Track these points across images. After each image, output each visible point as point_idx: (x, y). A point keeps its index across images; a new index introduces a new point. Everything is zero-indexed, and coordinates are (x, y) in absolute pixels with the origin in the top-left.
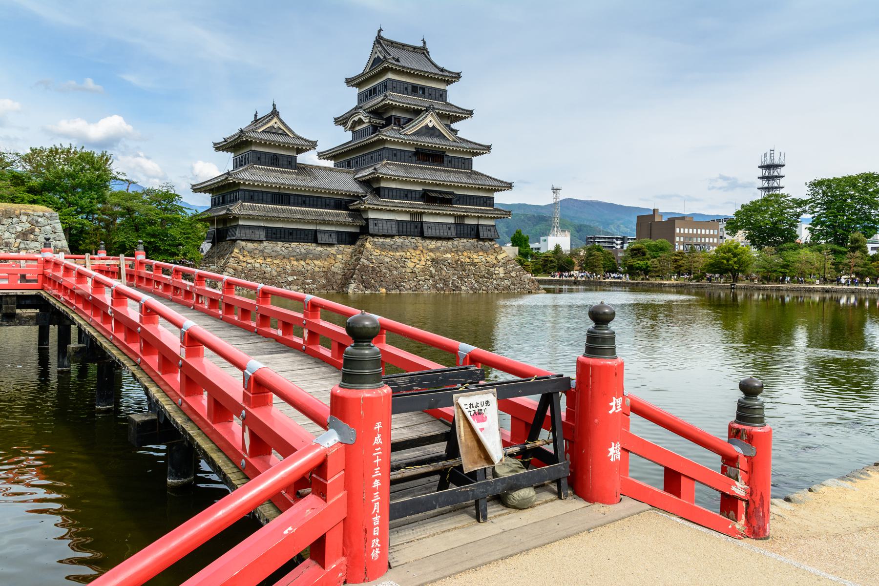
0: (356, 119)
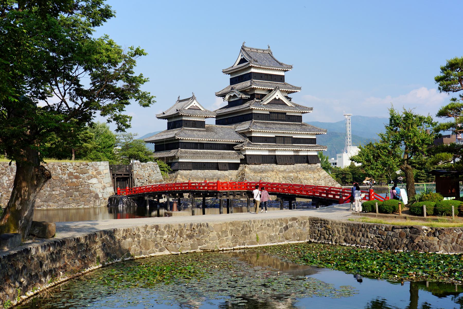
0: (232, 95)
